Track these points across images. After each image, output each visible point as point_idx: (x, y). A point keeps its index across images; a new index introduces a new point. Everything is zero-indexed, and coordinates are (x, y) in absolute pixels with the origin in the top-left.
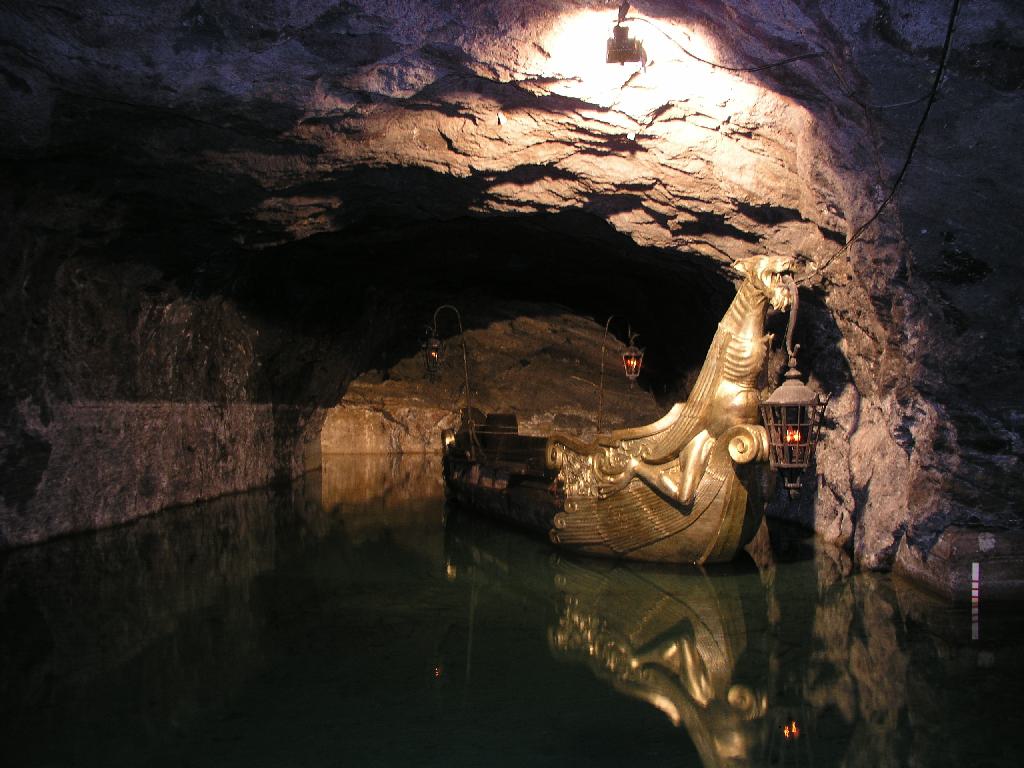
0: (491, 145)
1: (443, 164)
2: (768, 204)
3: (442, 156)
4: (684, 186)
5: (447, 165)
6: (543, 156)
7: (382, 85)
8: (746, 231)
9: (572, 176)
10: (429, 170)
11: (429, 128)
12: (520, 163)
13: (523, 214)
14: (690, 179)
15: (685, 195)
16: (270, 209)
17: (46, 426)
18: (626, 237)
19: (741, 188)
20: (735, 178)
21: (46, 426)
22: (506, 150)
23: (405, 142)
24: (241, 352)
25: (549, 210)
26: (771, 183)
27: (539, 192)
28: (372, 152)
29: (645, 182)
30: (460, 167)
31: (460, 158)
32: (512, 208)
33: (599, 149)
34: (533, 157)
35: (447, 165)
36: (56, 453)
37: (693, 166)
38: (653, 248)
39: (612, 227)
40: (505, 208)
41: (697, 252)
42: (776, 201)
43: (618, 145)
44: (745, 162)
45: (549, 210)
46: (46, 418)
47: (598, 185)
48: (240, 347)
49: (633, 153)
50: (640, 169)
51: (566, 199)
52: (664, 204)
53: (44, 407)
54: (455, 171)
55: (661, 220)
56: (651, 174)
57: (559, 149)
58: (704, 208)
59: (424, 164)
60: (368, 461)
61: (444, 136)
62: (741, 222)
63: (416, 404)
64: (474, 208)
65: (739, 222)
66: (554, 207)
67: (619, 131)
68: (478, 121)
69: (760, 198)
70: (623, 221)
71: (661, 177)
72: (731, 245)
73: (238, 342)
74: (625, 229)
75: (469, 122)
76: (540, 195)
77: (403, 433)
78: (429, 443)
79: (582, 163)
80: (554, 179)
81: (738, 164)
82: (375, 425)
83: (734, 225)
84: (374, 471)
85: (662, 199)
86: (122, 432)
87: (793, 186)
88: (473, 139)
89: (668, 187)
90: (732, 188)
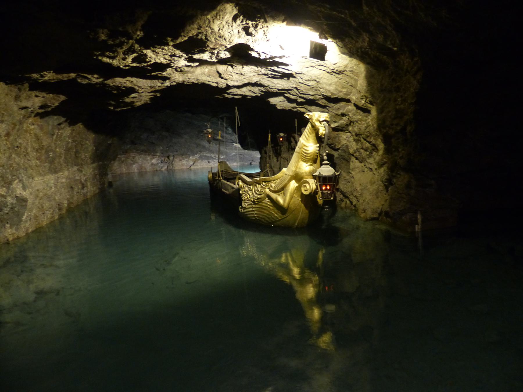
0: (237, 75)
1: (216, 83)
2: (338, 97)
3: (216, 80)
4: (305, 90)
5: (217, 83)
6: (255, 80)
8: (324, 105)
9: (261, 85)
10: (209, 85)
12: (246, 82)
13: (237, 98)
14: (309, 87)
15: (305, 93)
16: (134, 98)
17: (25, 191)
18: (274, 106)
19: (329, 91)
20: (328, 88)
21: (25, 191)
22: (242, 78)
23: (202, 74)
25: (247, 97)
26: (341, 90)
27: (245, 91)
28: (189, 79)
29: (291, 88)
30: (222, 84)
31: (223, 81)
32: (233, 96)
33: (277, 77)
34: (252, 80)
35: (217, 83)
36: (30, 202)
37: (311, 83)
38: (283, 109)
39: (269, 102)
40: (230, 96)
41: (299, 111)
42: (341, 95)
43: (288, 76)
44: (332, 81)
45: (247, 97)
46: (24, 188)
47: (271, 89)
49: (288, 79)
50: (290, 84)
51: (255, 93)
52: (294, 95)
53: (23, 184)
54: (220, 86)
55: (290, 100)
56: (294, 86)
57: (262, 77)
58: (311, 97)
61: (218, 72)
62: (323, 102)
64: (216, 96)
67: (290, 72)
68: (234, 67)
69: (335, 95)
70: (273, 100)
71: (298, 87)
74: (275, 103)
75: (230, 67)
76: (245, 92)
79: (267, 81)
80: (252, 86)
81: (329, 83)
83: (319, 103)
85: (294, 94)
86: (53, 188)
87: (349, 91)
89: (299, 91)
90: (326, 91)
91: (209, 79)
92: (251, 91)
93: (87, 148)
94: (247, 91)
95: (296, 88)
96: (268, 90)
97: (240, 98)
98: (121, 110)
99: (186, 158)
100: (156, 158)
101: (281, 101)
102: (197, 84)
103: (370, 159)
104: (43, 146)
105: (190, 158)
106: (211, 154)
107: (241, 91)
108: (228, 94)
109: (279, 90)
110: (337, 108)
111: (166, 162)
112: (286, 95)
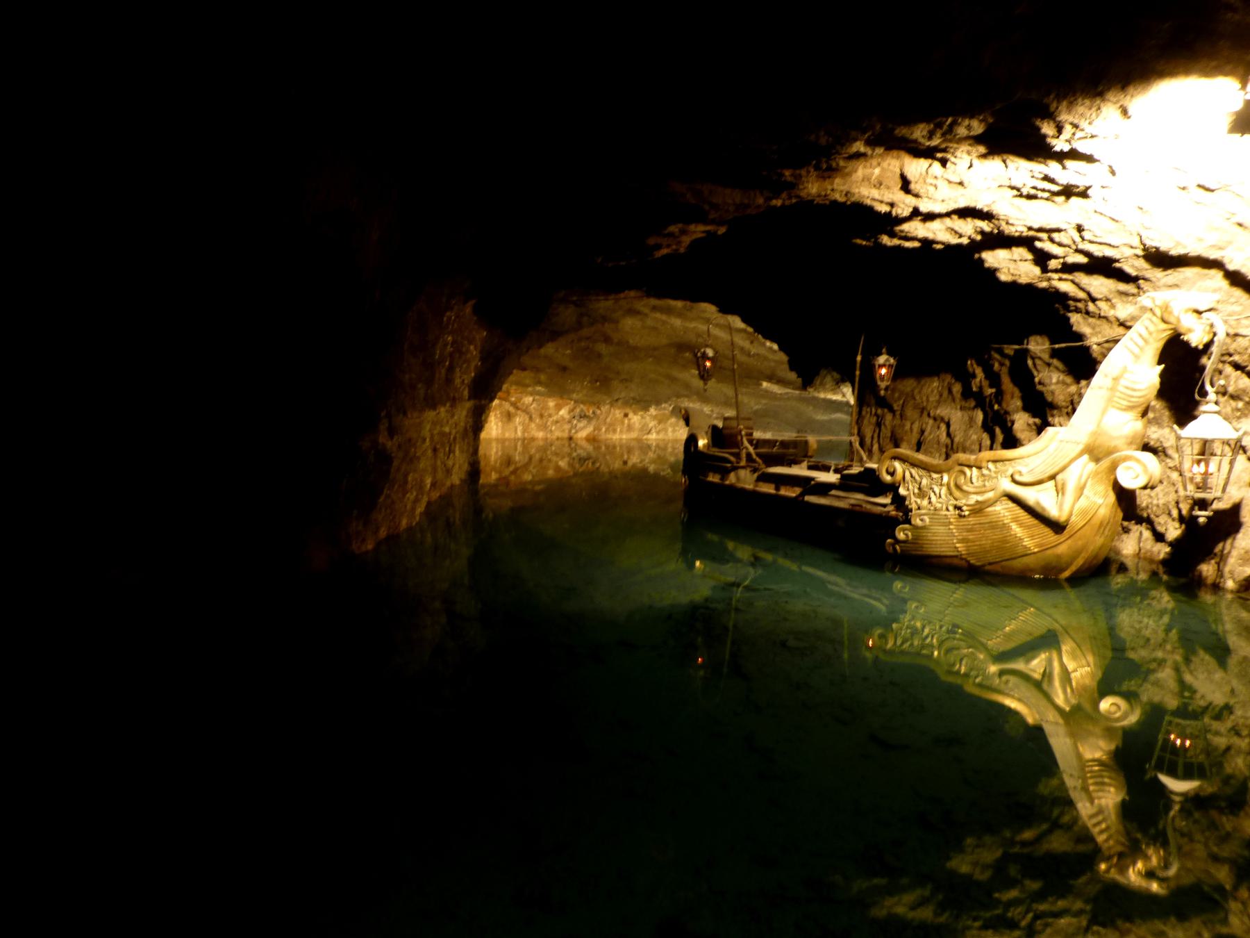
3: (891, 196)
7: (925, 133)
11: (891, 167)
13: (907, 249)
17: (392, 438)
18: (993, 272)
27: (939, 232)
28: (833, 190)
30: (904, 205)
35: (892, 205)
39: (981, 261)
40: (896, 242)
48: (472, 347)
55: (1042, 259)
59: (868, 202)
60: (494, 445)
63: (539, 393)
65: (1133, 266)
66: (943, 243)
70: (995, 258)
72: (1099, 285)
73: (470, 343)
75: (937, 165)
76: (937, 232)
77: (527, 421)
78: (551, 431)
82: (501, 413)
84: (500, 453)
85: (1066, 241)
86: (428, 440)
88: (934, 182)
91: (875, 193)
92: (952, 229)
94: (940, 230)
95: (1080, 229)
96: (998, 229)
97: (914, 249)
101: (1015, 261)
102: (844, 203)
103: (1243, 420)
105: (648, 411)
106: (703, 405)
107: (928, 229)
108: (892, 235)
109: (1030, 229)
110: (1170, 283)
111: (592, 416)
112: (1038, 244)
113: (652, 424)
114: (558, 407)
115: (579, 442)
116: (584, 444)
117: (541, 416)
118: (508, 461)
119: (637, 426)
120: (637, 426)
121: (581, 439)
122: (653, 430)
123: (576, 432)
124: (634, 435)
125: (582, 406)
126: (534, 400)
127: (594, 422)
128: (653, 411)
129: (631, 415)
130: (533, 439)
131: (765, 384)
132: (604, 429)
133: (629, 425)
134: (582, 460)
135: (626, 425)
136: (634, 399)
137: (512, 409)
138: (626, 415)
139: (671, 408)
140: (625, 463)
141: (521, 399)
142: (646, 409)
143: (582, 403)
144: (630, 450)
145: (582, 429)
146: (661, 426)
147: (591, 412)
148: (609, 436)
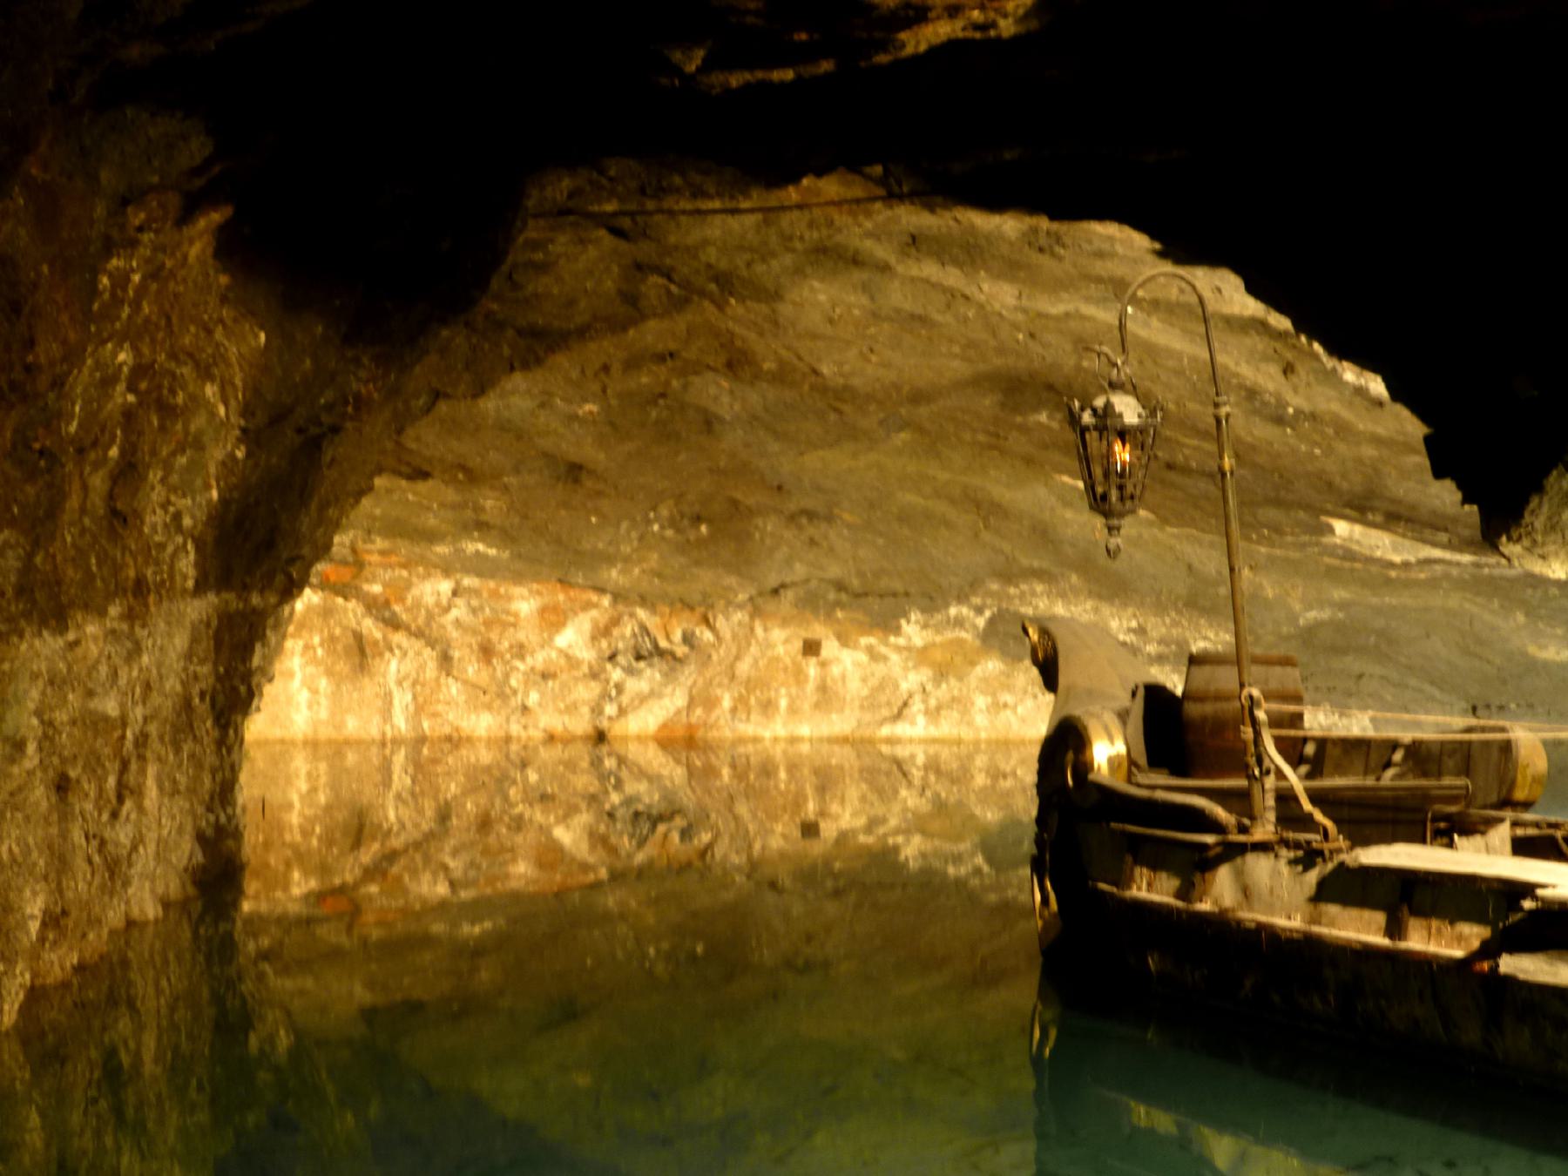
24: (213, 414)
48: (210, 390)
60: (300, 763)
63: (480, 566)
73: (205, 374)
77: (431, 670)
78: (525, 709)
82: (332, 639)
84: (322, 798)
86: (31, 748)
93: (199, 446)
98: (747, 86)
99: (868, 629)
100: (588, 606)
104: (28, 369)
105: (897, 631)
106: (1106, 610)
111: (681, 650)
113: (912, 679)
114: (553, 619)
115: (633, 751)
116: (653, 758)
117: (486, 652)
118: (359, 828)
119: (855, 687)
120: (855, 687)
121: (640, 739)
122: (917, 706)
123: (622, 712)
124: (841, 723)
125: (642, 613)
126: (455, 593)
127: (689, 675)
128: (913, 631)
129: (830, 648)
130: (455, 741)
131: (1341, 527)
132: (727, 703)
133: (823, 688)
134: (646, 820)
135: (811, 687)
136: (840, 586)
137: (371, 628)
138: (811, 648)
139: (981, 622)
140: (810, 830)
141: (408, 585)
142: (887, 624)
143: (644, 601)
144: (826, 780)
145: (643, 699)
146: (942, 692)
147: (677, 635)
148: (747, 729)
